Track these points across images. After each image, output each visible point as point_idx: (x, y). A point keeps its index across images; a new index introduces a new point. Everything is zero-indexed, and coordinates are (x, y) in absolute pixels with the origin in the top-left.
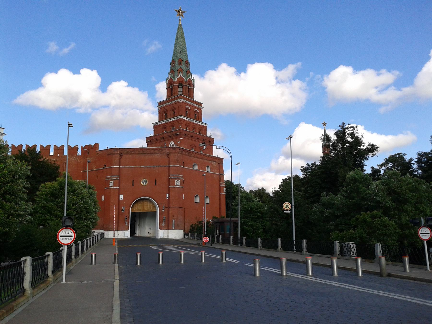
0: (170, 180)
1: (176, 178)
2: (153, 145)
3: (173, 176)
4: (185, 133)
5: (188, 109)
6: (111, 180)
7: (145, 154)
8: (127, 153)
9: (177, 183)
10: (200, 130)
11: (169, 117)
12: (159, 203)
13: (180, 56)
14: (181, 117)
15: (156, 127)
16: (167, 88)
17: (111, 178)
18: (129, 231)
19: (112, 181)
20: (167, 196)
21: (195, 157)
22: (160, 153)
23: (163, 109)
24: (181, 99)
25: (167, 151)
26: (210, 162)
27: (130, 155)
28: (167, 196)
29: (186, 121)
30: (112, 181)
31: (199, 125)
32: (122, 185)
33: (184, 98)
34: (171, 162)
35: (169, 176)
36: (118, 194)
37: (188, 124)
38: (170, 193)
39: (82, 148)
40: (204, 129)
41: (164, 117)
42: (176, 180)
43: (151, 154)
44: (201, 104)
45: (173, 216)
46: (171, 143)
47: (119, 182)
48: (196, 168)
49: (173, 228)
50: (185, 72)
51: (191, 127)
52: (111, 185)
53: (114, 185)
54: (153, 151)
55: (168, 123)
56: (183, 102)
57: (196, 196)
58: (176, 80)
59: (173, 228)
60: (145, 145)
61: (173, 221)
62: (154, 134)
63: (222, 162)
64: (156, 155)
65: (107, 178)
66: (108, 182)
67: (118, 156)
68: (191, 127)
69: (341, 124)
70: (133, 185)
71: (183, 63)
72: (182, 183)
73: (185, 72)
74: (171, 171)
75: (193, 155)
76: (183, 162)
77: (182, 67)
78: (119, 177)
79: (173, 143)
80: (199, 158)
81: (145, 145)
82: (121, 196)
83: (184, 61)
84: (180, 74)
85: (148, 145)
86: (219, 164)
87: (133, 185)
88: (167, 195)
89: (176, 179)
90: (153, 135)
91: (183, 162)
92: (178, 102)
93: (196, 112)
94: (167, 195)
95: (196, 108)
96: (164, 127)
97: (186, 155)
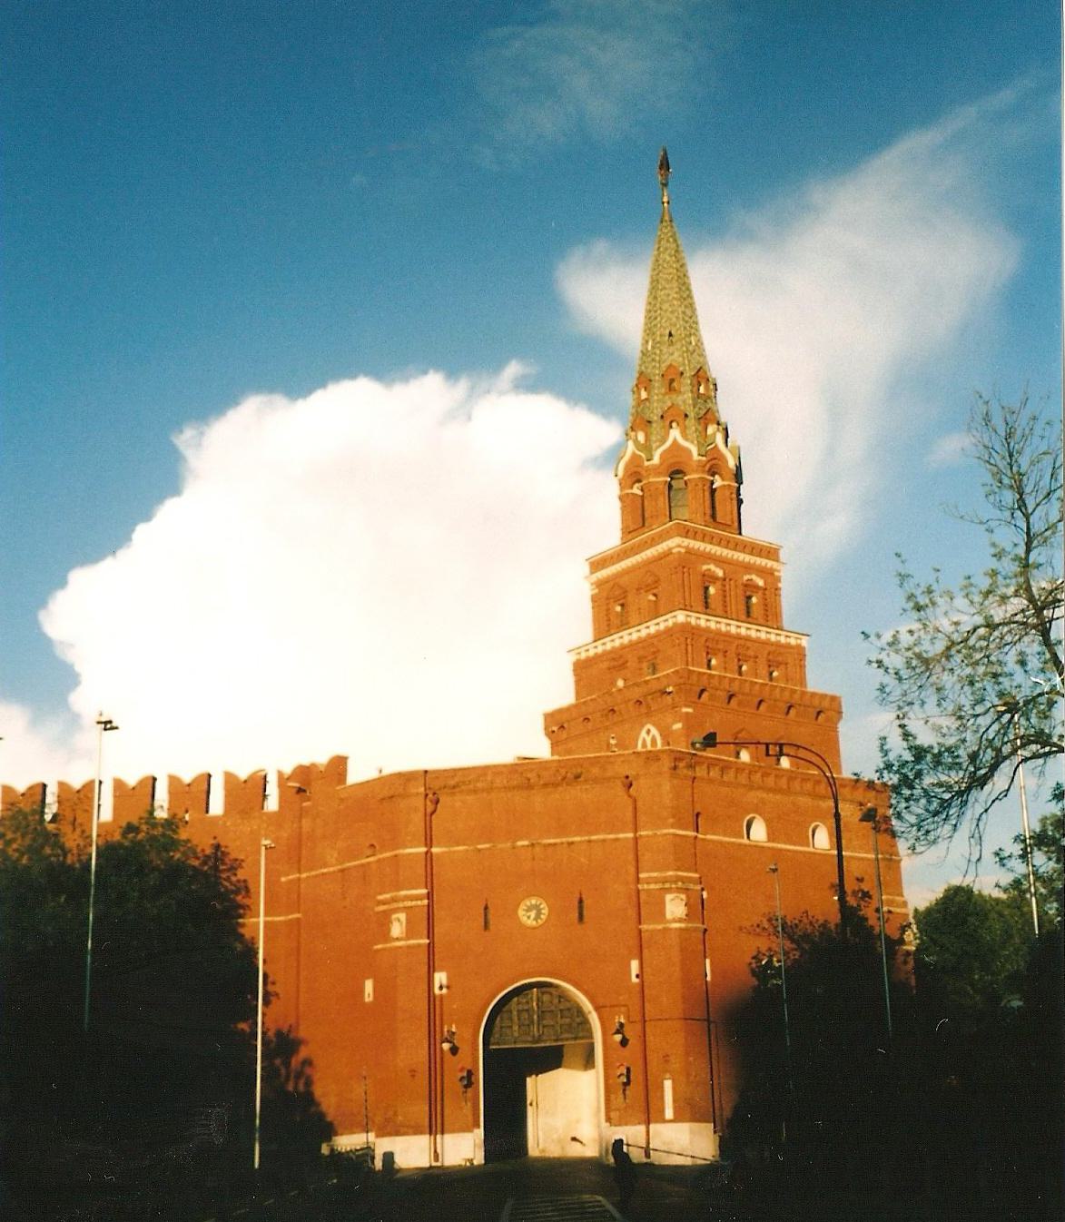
0: (643, 897)
2: (571, 745)
3: (656, 881)
5: (714, 579)
6: (396, 910)
10: (771, 665)
11: (634, 618)
12: (601, 1001)
13: (675, 356)
15: (582, 669)
16: (621, 498)
17: (394, 900)
18: (480, 1132)
19: (402, 916)
21: (751, 787)
23: (612, 583)
27: (470, 798)
29: (708, 630)
31: (767, 643)
33: (687, 533)
34: (642, 818)
35: (638, 880)
37: (713, 644)
39: (282, 780)
41: (615, 621)
42: (669, 897)
44: (771, 552)
45: (666, 1058)
46: (643, 734)
48: (759, 832)
49: (669, 1114)
50: (691, 422)
51: (732, 654)
52: (397, 930)
53: (410, 933)
55: (632, 645)
58: (656, 460)
59: (669, 1114)
60: (541, 749)
61: (668, 1084)
65: (383, 902)
66: (384, 921)
68: (732, 654)
71: (685, 384)
74: (646, 858)
77: (679, 400)
78: (429, 896)
79: (654, 731)
80: (770, 790)
81: (541, 749)
82: (440, 978)
84: (675, 433)
85: (555, 745)
87: (486, 926)
88: (635, 966)
89: (669, 890)
92: (668, 553)
93: (749, 586)
94: (635, 966)
95: (749, 568)
96: (616, 662)
97: (711, 781)
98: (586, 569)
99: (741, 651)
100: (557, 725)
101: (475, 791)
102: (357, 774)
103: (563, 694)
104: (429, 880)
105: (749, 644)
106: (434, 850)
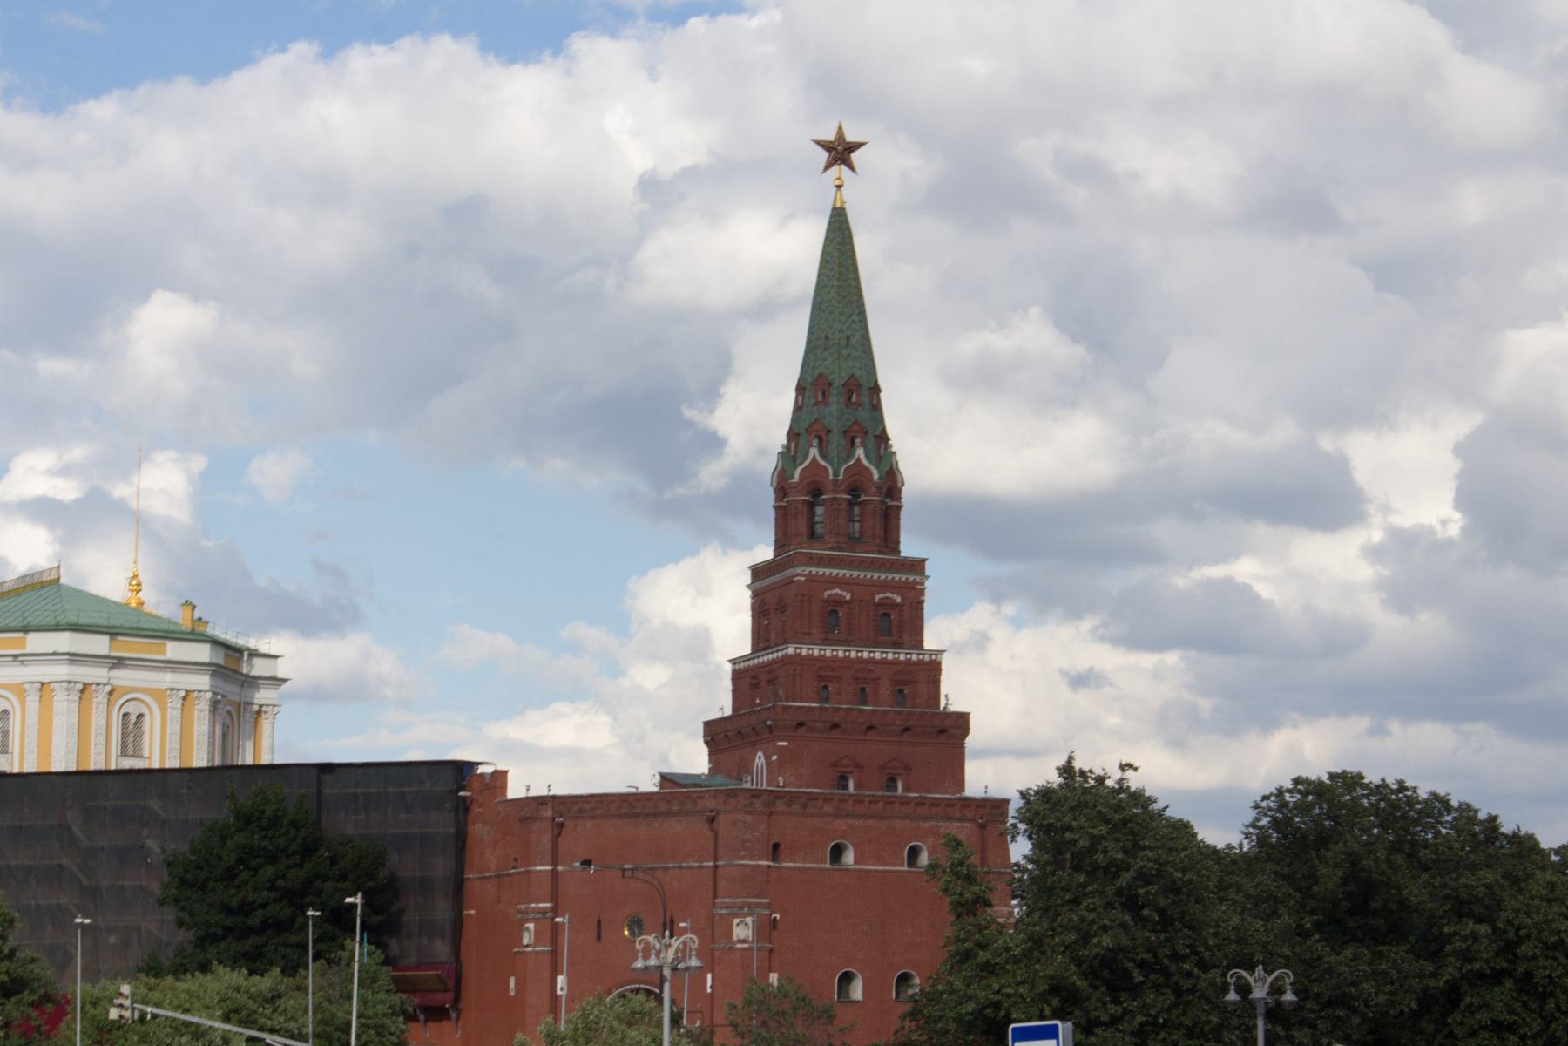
1: (737, 911)
3: (728, 906)
5: (840, 602)
6: (528, 921)
7: (636, 816)
9: (742, 931)
14: (791, 650)
15: (746, 678)
19: (531, 926)
20: (709, 983)
21: (838, 816)
24: (799, 570)
25: (710, 803)
26: (925, 825)
27: (589, 824)
28: (709, 983)
29: (822, 658)
30: (531, 926)
35: (714, 906)
36: (547, 974)
37: (826, 673)
38: (717, 969)
42: (736, 921)
43: (657, 815)
53: (538, 940)
54: (663, 807)
56: (811, 578)
57: (847, 978)
60: (695, 760)
62: (734, 709)
65: (519, 912)
66: (519, 928)
69: (1061, 761)
70: (599, 938)
72: (767, 928)
73: (835, 440)
74: (722, 884)
75: (828, 808)
76: (776, 846)
80: (864, 816)
83: (838, 382)
86: (983, 827)
87: (599, 938)
88: (709, 976)
89: (736, 915)
90: (728, 712)
91: (776, 846)
94: (709, 976)
95: (884, 586)
98: (748, 579)
99: (863, 678)
100: (716, 734)
101: (593, 818)
102: (514, 791)
103: (721, 703)
104: (554, 898)
105: (871, 667)
106: (560, 868)
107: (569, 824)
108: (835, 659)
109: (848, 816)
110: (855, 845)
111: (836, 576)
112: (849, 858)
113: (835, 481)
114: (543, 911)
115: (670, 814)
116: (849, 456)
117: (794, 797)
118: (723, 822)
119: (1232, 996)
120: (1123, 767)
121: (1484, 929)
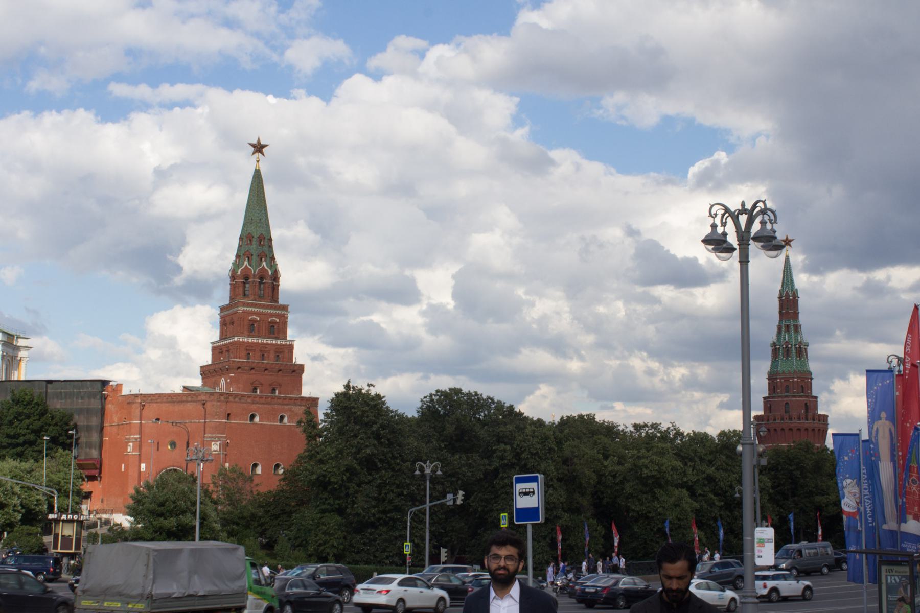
1: (213, 439)
4: (239, 365)
5: (256, 321)
8: (151, 402)
9: (215, 447)
14: (236, 339)
15: (217, 350)
19: (131, 444)
22: (194, 401)
25: (203, 398)
29: (248, 342)
32: (143, 450)
40: (286, 351)
43: (182, 402)
47: (140, 446)
53: (134, 450)
54: (184, 398)
56: (244, 312)
57: (255, 466)
60: (197, 382)
63: (317, 403)
64: (188, 405)
67: (138, 405)
69: (345, 383)
73: (255, 259)
74: (207, 429)
75: (249, 400)
76: (229, 415)
82: (143, 466)
83: (256, 236)
90: (210, 363)
91: (229, 415)
95: (272, 315)
99: (263, 350)
100: (205, 372)
102: (125, 391)
104: (140, 433)
107: (147, 405)
108: (253, 343)
109: (257, 403)
110: (260, 415)
111: (251, 310)
112: (257, 419)
113: (254, 275)
114: (136, 439)
115: (187, 401)
116: (260, 265)
117: (236, 396)
118: (208, 405)
119: (417, 472)
120: (369, 385)
121: (508, 447)
